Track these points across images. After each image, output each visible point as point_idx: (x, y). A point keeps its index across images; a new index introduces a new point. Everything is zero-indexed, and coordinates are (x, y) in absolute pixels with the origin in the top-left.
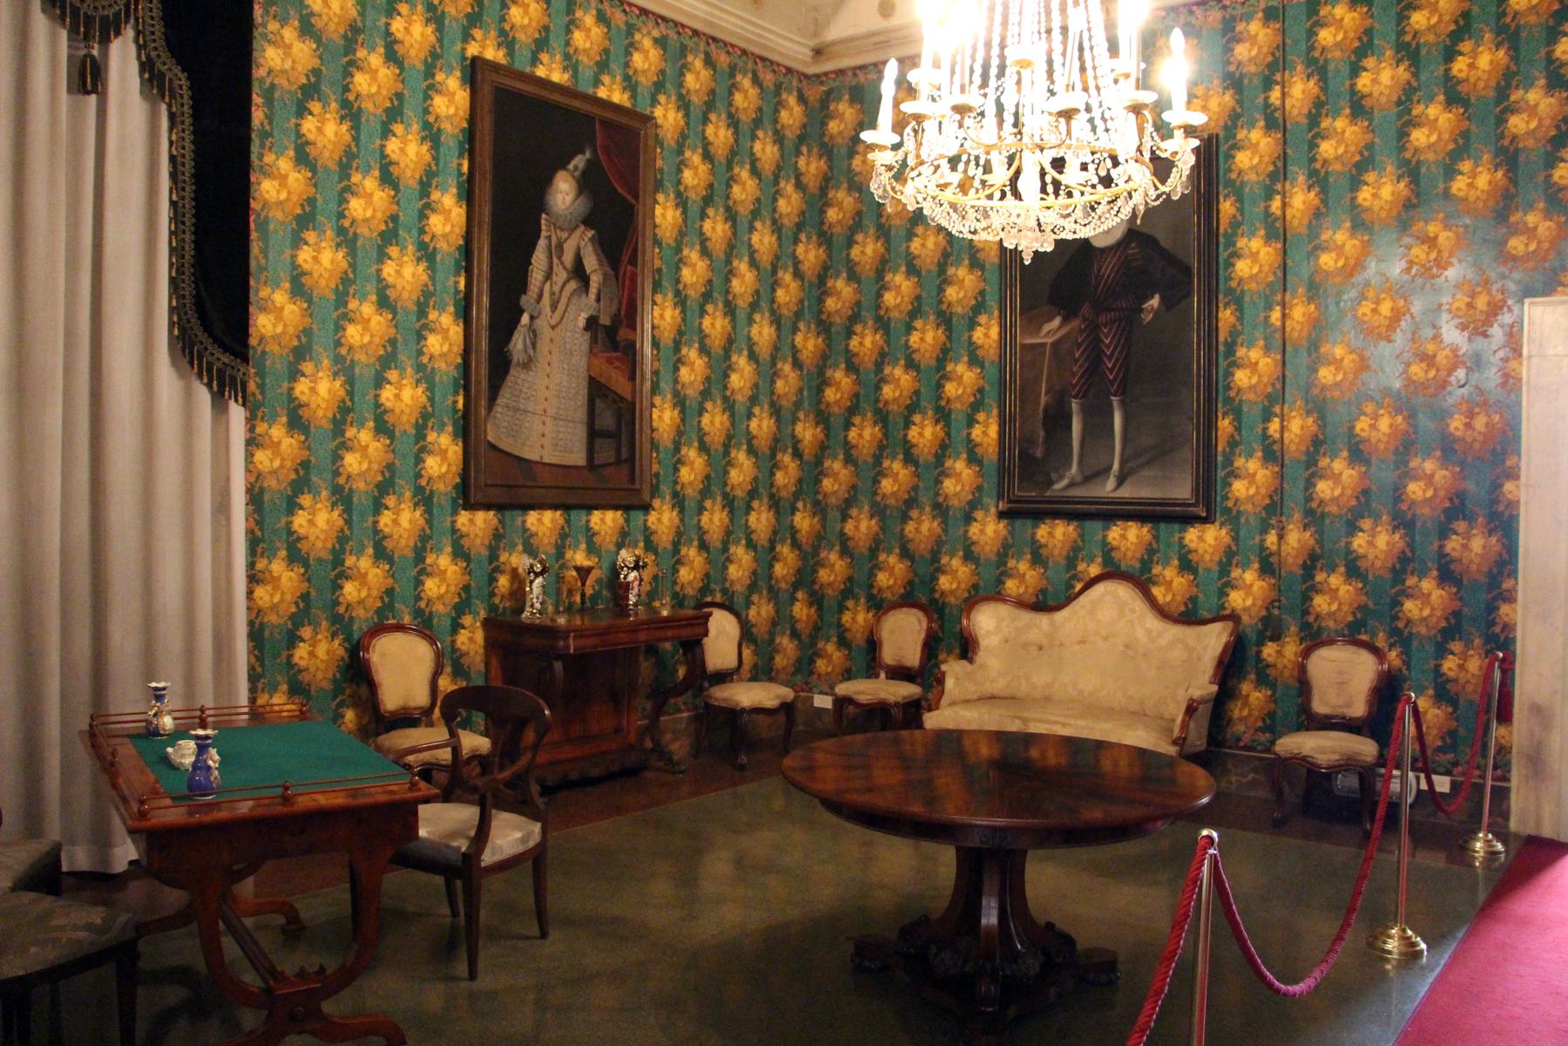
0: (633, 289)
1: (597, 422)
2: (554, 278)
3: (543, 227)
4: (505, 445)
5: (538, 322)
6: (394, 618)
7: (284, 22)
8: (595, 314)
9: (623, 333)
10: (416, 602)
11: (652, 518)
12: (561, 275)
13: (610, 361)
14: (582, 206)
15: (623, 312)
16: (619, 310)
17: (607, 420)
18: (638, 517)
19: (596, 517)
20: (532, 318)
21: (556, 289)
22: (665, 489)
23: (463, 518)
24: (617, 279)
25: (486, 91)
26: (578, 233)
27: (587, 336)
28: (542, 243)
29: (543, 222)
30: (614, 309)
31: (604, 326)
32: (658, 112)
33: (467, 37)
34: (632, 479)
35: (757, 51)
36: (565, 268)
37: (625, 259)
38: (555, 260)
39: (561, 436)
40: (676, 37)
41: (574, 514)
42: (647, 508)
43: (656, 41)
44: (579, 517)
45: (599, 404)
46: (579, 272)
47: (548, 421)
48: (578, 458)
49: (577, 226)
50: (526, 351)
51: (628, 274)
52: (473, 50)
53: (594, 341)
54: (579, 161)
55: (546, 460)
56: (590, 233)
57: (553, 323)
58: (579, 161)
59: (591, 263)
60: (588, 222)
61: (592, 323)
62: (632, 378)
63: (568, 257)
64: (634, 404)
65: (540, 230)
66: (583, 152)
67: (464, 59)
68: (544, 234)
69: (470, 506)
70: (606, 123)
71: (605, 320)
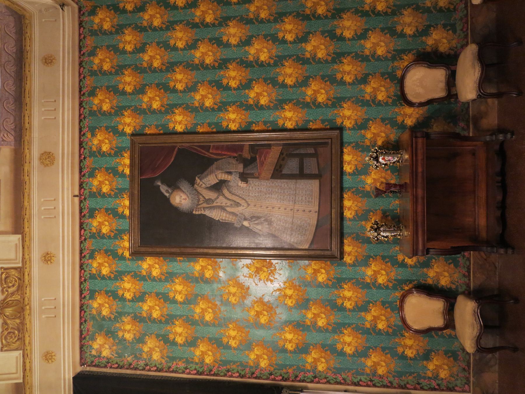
0: (222, 148)
1: (294, 172)
2: (223, 204)
3: (200, 213)
4: (311, 237)
5: (247, 215)
6: (396, 302)
7: (142, 351)
8: (238, 175)
9: (246, 155)
10: (389, 289)
11: (348, 124)
12: (221, 201)
13: (262, 164)
14: (184, 185)
15: (235, 155)
16: (234, 157)
17: (292, 165)
18: (347, 136)
19: (347, 168)
20: (245, 219)
21: (229, 203)
22: (330, 114)
23: (348, 259)
24: (220, 159)
25: (143, 249)
26: (199, 189)
27: (250, 180)
28: (207, 213)
29: (197, 213)
30: (234, 161)
31: (244, 168)
32: (128, 130)
33: (122, 258)
34: (326, 144)
35: (77, 53)
36: (218, 198)
37: (207, 154)
38: (215, 204)
39: (304, 198)
40: (87, 120)
41: (346, 185)
42: (341, 129)
44: (348, 181)
45: (285, 171)
46: (218, 187)
47: (296, 207)
48: (314, 185)
49: (196, 190)
50: (261, 223)
51: (215, 152)
52: (127, 254)
53: (252, 176)
54: (164, 189)
55: (317, 209)
56: (198, 180)
57: (246, 205)
58: (164, 189)
59: (211, 179)
60: (192, 183)
61: (244, 177)
62: (269, 146)
63: (211, 195)
64: (284, 145)
65: (201, 214)
66: (159, 186)
67: (132, 260)
68: (203, 212)
69: (342, 253)
70: (142, 173)
71: (240, 168)
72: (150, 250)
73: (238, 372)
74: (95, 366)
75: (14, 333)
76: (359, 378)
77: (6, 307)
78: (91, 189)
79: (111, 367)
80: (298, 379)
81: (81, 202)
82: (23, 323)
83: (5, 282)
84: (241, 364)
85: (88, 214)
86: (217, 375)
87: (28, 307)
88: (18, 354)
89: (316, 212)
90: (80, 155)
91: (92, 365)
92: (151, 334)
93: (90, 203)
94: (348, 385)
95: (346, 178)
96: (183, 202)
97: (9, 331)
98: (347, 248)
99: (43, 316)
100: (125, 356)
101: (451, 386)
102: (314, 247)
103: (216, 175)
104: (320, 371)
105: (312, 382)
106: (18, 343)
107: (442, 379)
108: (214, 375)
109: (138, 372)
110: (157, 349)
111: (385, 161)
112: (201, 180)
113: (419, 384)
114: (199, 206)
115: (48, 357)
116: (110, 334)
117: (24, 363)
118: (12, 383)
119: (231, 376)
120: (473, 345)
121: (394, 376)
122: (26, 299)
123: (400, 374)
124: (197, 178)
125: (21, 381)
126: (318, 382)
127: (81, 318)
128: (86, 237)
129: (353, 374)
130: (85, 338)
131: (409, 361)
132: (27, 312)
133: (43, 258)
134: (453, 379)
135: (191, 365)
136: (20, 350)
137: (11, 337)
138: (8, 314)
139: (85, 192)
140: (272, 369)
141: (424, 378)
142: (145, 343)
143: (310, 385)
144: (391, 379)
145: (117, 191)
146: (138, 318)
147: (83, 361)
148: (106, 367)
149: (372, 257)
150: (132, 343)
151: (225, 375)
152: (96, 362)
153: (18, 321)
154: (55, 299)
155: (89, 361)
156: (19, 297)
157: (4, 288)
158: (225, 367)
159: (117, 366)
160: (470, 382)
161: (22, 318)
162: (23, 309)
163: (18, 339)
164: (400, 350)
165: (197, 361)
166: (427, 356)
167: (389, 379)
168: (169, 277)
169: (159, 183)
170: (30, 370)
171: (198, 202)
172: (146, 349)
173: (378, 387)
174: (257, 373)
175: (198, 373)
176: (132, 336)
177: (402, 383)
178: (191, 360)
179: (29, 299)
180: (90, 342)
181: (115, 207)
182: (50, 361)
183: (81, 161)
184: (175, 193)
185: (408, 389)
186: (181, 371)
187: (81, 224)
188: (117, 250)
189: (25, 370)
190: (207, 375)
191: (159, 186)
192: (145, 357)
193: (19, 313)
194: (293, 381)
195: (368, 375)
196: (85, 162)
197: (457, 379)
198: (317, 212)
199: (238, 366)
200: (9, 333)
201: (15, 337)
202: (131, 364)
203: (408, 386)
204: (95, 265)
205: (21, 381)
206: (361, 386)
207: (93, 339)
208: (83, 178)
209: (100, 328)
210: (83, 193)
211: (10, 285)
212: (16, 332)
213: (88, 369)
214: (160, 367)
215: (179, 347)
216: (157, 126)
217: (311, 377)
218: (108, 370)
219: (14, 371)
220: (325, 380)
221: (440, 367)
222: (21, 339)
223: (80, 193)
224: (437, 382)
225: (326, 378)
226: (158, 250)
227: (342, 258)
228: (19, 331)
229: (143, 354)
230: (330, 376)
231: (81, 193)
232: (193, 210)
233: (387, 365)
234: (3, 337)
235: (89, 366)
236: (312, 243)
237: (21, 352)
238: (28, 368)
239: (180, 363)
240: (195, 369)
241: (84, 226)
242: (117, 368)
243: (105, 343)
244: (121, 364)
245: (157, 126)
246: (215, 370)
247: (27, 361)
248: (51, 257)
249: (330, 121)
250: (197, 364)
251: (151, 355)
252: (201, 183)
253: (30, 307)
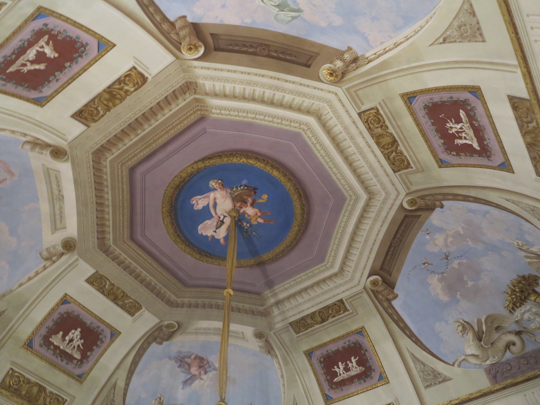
75: (17, 385)
77: (39, 389)
82: (19, 395)
83: (56, 398)
106: (8, 383)
138: (34, 388)
153: (24, 393)
156: (39, 403)
157: (53, 395)
201: (13, 384)
211: (52, 401)
212: (16, 387)
234: (20, 376)
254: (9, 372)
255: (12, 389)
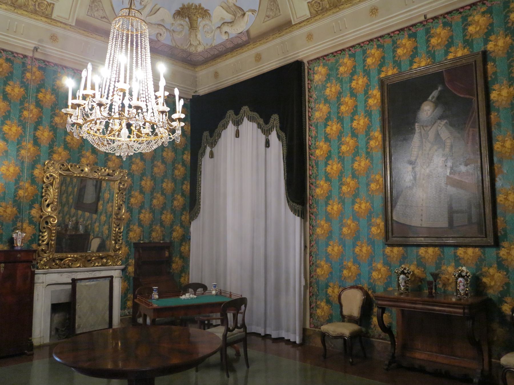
4: (402, 221)
6: (361, 284)
18: (491, 252)
23: (388, 249)
26: (436, 125)
29: (416, 127)
32: (490, 46)
33: (380, 72)
43: (483, 13)
52: (383, 75)
54: (435, 93)
58: (435, 93)
69: (392, 245)
72: (386, 94)
73: (312, 174)
74: (308, 72)
75: (320, 7)
76: (314, 256)
78: (433, 28)
79: (308, 84)
80: (311, 215)
81: (421, 23)
82: (327, 10)
84: (317, 176)
85: (411, 32)
86: (310, 159)
87: (338, 10)
88: (308, 15)
89: (421, 225)
90: (462, 8)
91: (309, 69)
92: (330, 108)
93: (421, 31)
94: (310, 249)
95: (452, 249)
96: (425, 113)
97: (321, 3)
98: (396, 249)
99: (334, 24)
100: (315, 92)
101: (313, 315)
102: (395, 225)
103: (449, 138)
104: (316, 230)
105: (310, 224)
107: (316, 311)
108: (310, 157)
109: (307, 104)
110: (322, 114)
111: (459, 283)
112: (444, 125)
113: (313, 295)
114: (422, 128)
115: (310, 37)
116: (328, 77)
117: (304, 21)
118: (291, 18)
119: (309, 170)
120: (325, 330)
121: (316, 279)
122: (343, 6)
123: (317, 283)
124: (445, 121)
125: (293, 23)
126: (310, 229)
127: (336, 52)
128: (393, 37)
129: (316, 252)
130: (324, 59)
131: (325, 290)
132: (334, 10)
133: (373, 8)
134: (316, 318)
135: (314, 141)
136: (311, 15)
137: (317, 6)
139: (430, 24)
140: (315, 197)
141: (316, 299)
142: (325, 105)
143: (308, 223)
144: (315, 277)
145: (433, 52)
146: (339, 95)
147: (310, 62)
148: (308, 80)
149: (390, 268)
150: (324, 95)
151: (310, 165)
152: (311, 72)
153: (328, 6)
154: (346, 28)
155: (311, 66)
158: (314, 164)
159: (310, 87)
160: (316, 328)
161: (330, 9)
162: (336, 6)
163: (317, 11)
164: (331, 284)
165: (317, 144)
166: (328, 302)
167: (314, 276)
168: (369, 114)
169: (439, 89)
170: (301, 27)
171: (425, 126)
172: (321, 106)
173: (310, 268)
174: (313, 187)
175: (310, 146)
176: (328, 94)
177: (312, 284)
178: (317, 140)
179: (343, 9)
180: (322, 64)
181: (419, 55)
182: (307, 39)
183: (457, 10)
184: (432, 104)
185: (310, 287)
186: (310, 134)
187: (402, 30)
188: (385, 66)
189: (300, 24)
190: (309, 153)
191: (437, 89)
192: (316, 107)
193: (333, 5)
194: (310, 211)
195: (316, 262)
196: (457, 14)
197: (316, 320)
198: (421, 225)
199: (316, 173)
200: (319, 3)
201: (318, 9)
202: (311, 97)
203: (311, 288)
204: (373, 51)
205: (293, 23)
206: (310, 257)
207: (324, 65)
208: (442, 17)
209: (331, 69)
210: (429, 22)
212: (321, 8)
213: (306, 67)
214: (311, 119)
215: (324, 130)
216: (495, 73)
217: (313, 223)
218: (307, 82)
219: (298, 17)
220: (311, 234)
221: (323, 310)
222: (317, 14)
223: (428, 19)
224: (315, 307)
225: (313, 234)
226: (386, 101)
227: (389, 245)
228: (321, 10)
229: (318, 105)
230: (314, 237)
231: (428, 21)
232: (418, 123)
233: (322, 275)
235: (308, 68)
236: (397, 222)
237: (310, 17)
238: (301, 25)
239: (315, 132)
240: (312, 144)
241: (402, 32)
242: (308, 88)
243: (322, 75)
244: (311, 91)
245: (495, 73)
246: (312, 157)
247: (305, 23)
248: (375, 13)
249: (505, 235)
250: (315, 144)
251: (318, 111)
252: (441, 125)
253: (338, 11)
254: (308, 5)
255: (319, 12)
